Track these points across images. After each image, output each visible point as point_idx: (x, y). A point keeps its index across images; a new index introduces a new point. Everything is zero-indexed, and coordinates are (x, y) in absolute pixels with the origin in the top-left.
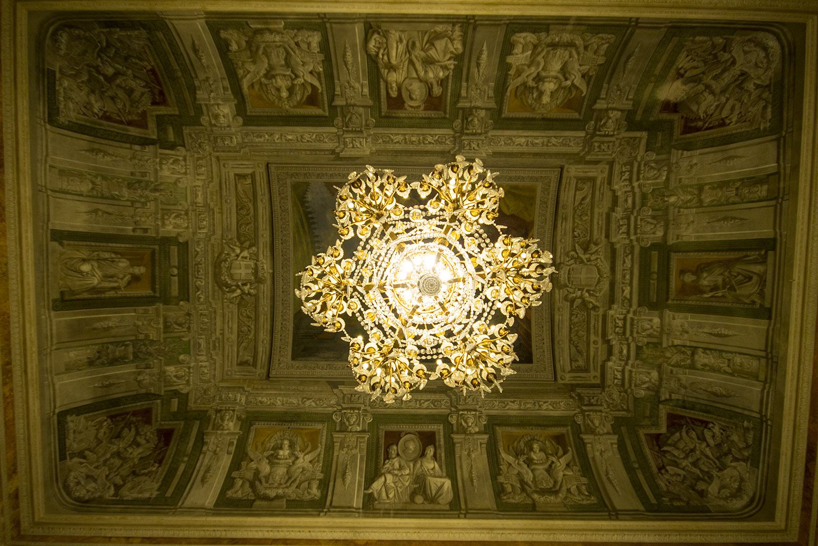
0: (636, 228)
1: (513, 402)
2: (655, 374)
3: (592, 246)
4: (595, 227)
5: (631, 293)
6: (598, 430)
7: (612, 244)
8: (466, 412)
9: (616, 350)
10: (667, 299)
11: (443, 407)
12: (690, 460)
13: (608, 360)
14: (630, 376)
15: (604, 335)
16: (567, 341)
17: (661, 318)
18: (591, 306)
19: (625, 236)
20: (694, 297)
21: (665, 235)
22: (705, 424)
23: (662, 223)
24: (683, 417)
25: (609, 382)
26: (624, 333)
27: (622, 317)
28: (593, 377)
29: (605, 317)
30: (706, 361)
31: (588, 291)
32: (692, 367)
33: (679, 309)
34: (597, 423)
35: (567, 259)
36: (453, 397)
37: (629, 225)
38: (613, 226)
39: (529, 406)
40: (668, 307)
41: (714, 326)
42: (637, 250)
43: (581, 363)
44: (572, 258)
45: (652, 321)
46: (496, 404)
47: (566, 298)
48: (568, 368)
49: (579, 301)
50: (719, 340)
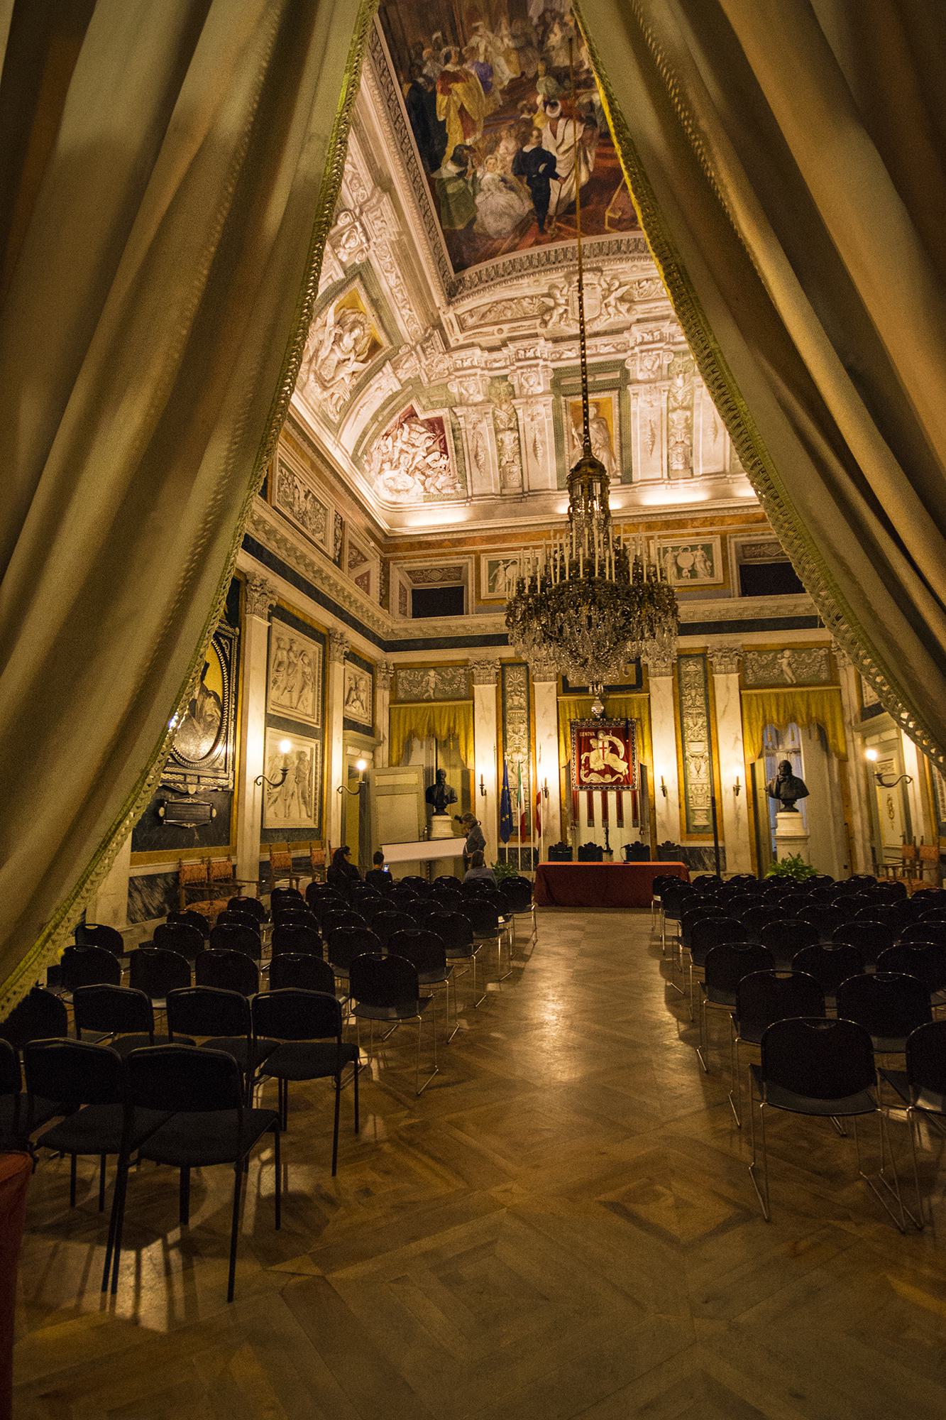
0: (648, 350)
1: (397, 277)
2: (480, 398)
3: (627, 306)
4: (652, 305)
5: (568, 359)
6: (400, 371)
7: (628, 328)
8: (360, 229)
9: (496, 355)
10: (565, 395)
11: (354, 194)
12: (404, 447)
13: (482, 349)
14: (470, 375)
15: (512, 339)
16: (495, 298)
17: (543, 394)
18: (546, 317)
19: (639, 340)
20: (570, 419)
21: (638, 382)
22: (444, 451)
23: (652, 376)
24: (443, 431)
25: (456, 355)
26: (519, 360)
27: (538, 354)
28: (456, 337)
29: (536, 336)
30: (507, 442)
31: (566, 311)
32: (497, 431)
33: (556, 407)
34: (407, 365)
35: (608, 279)
36: (374, 201)
37: (653, 342)
38: (651, 326)
39: (399, 296)
40: (557, 397)
41: (543, 443)
42: (621, 356)
43: (470, 321)
44: (610, 285)
45: (538, 383)
46: (388, 259)
47: (553, 286)
48: (459, 312)
49: (551, 303)
50: (530, 449)
